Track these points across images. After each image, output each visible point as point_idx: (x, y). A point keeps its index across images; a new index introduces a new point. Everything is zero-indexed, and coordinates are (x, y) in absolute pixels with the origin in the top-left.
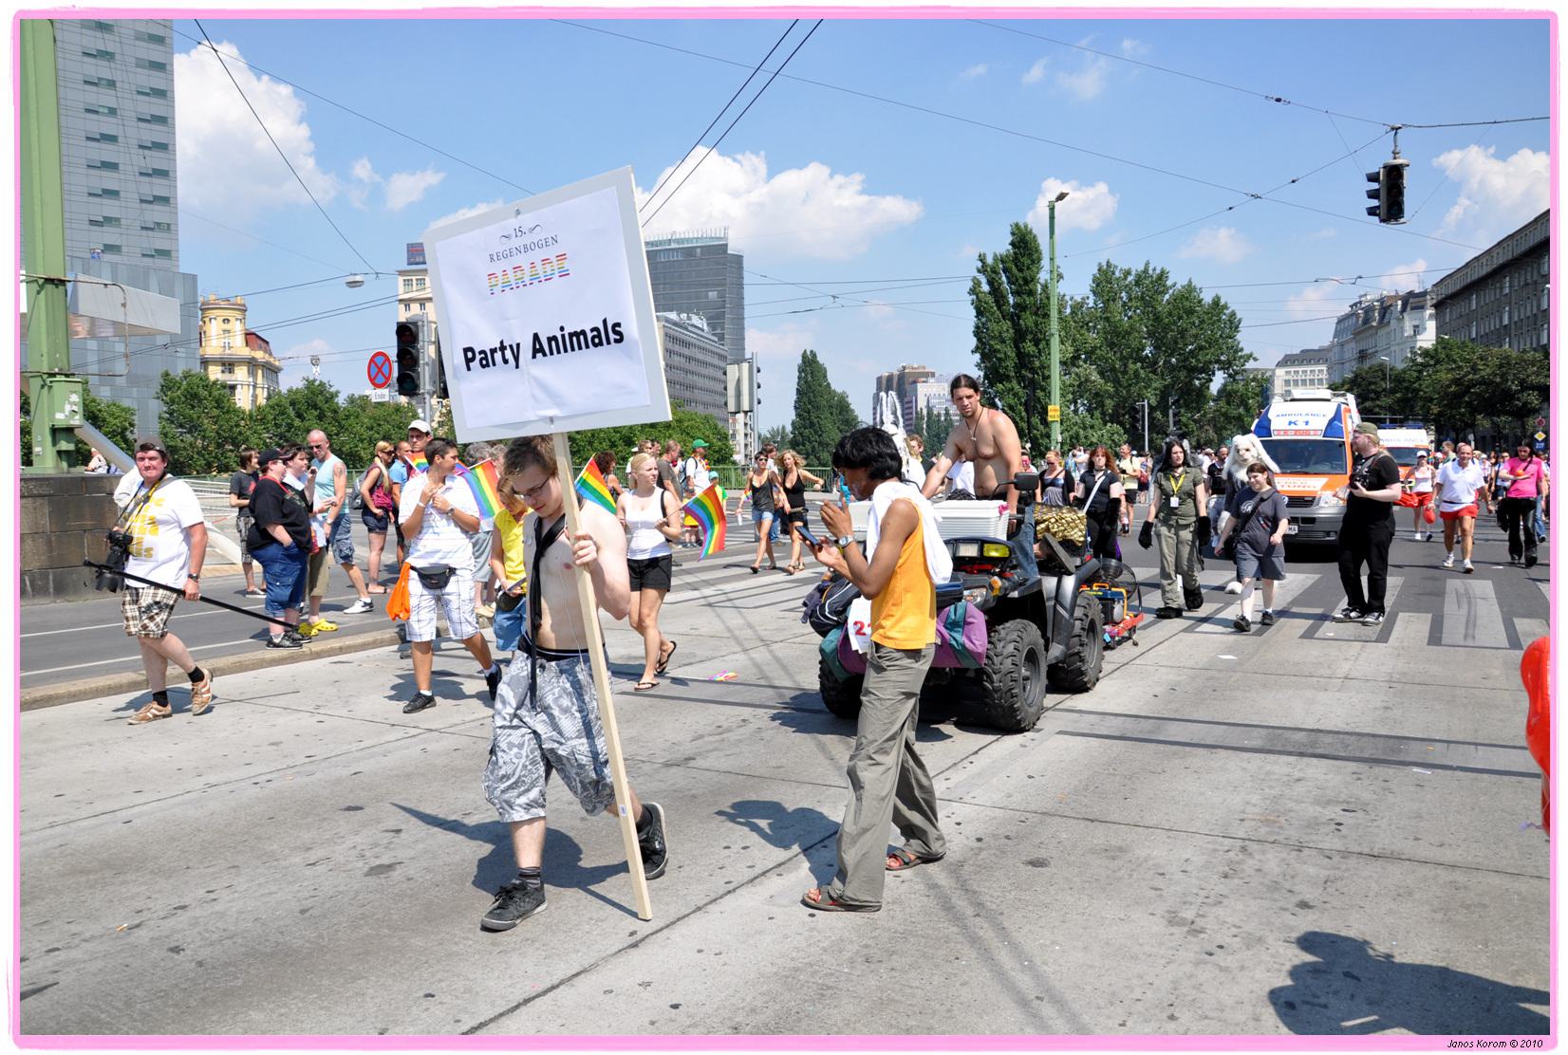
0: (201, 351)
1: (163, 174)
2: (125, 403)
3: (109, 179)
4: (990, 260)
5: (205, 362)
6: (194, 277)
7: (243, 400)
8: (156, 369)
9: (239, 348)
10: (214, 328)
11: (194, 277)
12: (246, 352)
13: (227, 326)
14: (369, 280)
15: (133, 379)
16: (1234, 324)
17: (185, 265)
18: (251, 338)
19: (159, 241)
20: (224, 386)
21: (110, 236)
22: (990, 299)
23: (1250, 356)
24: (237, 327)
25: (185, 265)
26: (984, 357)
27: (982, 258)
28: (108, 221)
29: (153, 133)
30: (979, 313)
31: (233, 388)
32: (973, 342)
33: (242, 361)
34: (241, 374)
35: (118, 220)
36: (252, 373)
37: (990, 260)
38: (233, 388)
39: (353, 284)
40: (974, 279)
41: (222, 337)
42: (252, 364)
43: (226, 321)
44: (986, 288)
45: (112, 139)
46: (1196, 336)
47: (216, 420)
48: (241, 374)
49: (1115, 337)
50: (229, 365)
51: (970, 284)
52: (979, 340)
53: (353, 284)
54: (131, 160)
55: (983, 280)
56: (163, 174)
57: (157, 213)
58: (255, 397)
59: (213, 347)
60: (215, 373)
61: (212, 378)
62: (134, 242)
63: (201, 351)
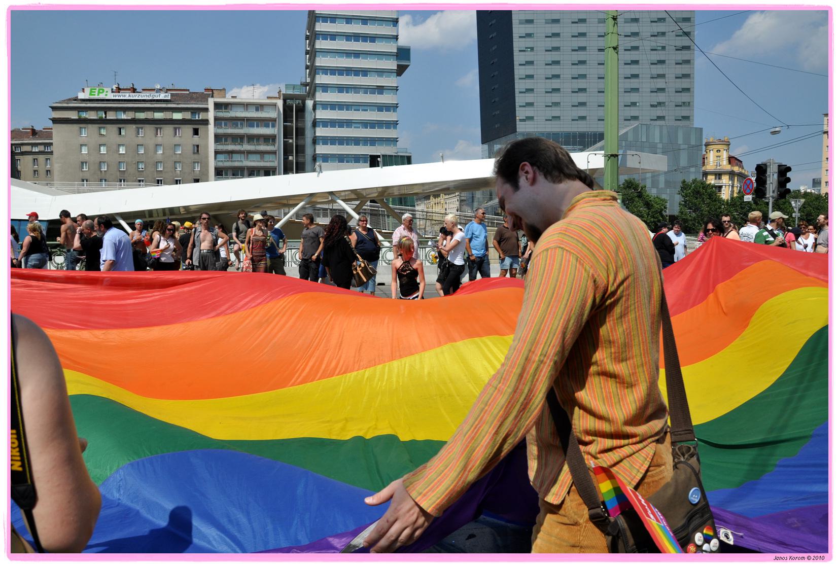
0: (703, 168)
1: (686, 76)
2: (663, 197)
3: (660, 83)
5: (706, 174)
6: (700, 130)
7: (725, 195)
8: (679, 178)
9: (725, 165)
10: (712, 156)
11: (700, 130)
12: (728, 168)
13: (718, 154)
15: (668, 183)
17: (697, 124)
18: (731, 160)
19: (684, 112)
20: (716, 187)
21: (659, 112)
24: (725, 155)
25: (697, 124)
28: (660, 104)
29: (685, 55)
31: (720, 187)
33: (725, 173)
34: (725, 180)
35: (664, 103)
36: (732, 179)
38: (720, 187)
41: (716, 159)
42: (732, 174)
43: (718, 151)
45: (662, 62)
47: (708, 205)
48: (725, 180)
50: (718, 175)
54: (671, 71)
56: (686, 76)
57: (684, 97)
58: (733, 192)
59: (711, 165)
60: (711, 180)
61: (708, 182)
62: (670, 113)
63: (703, 168)
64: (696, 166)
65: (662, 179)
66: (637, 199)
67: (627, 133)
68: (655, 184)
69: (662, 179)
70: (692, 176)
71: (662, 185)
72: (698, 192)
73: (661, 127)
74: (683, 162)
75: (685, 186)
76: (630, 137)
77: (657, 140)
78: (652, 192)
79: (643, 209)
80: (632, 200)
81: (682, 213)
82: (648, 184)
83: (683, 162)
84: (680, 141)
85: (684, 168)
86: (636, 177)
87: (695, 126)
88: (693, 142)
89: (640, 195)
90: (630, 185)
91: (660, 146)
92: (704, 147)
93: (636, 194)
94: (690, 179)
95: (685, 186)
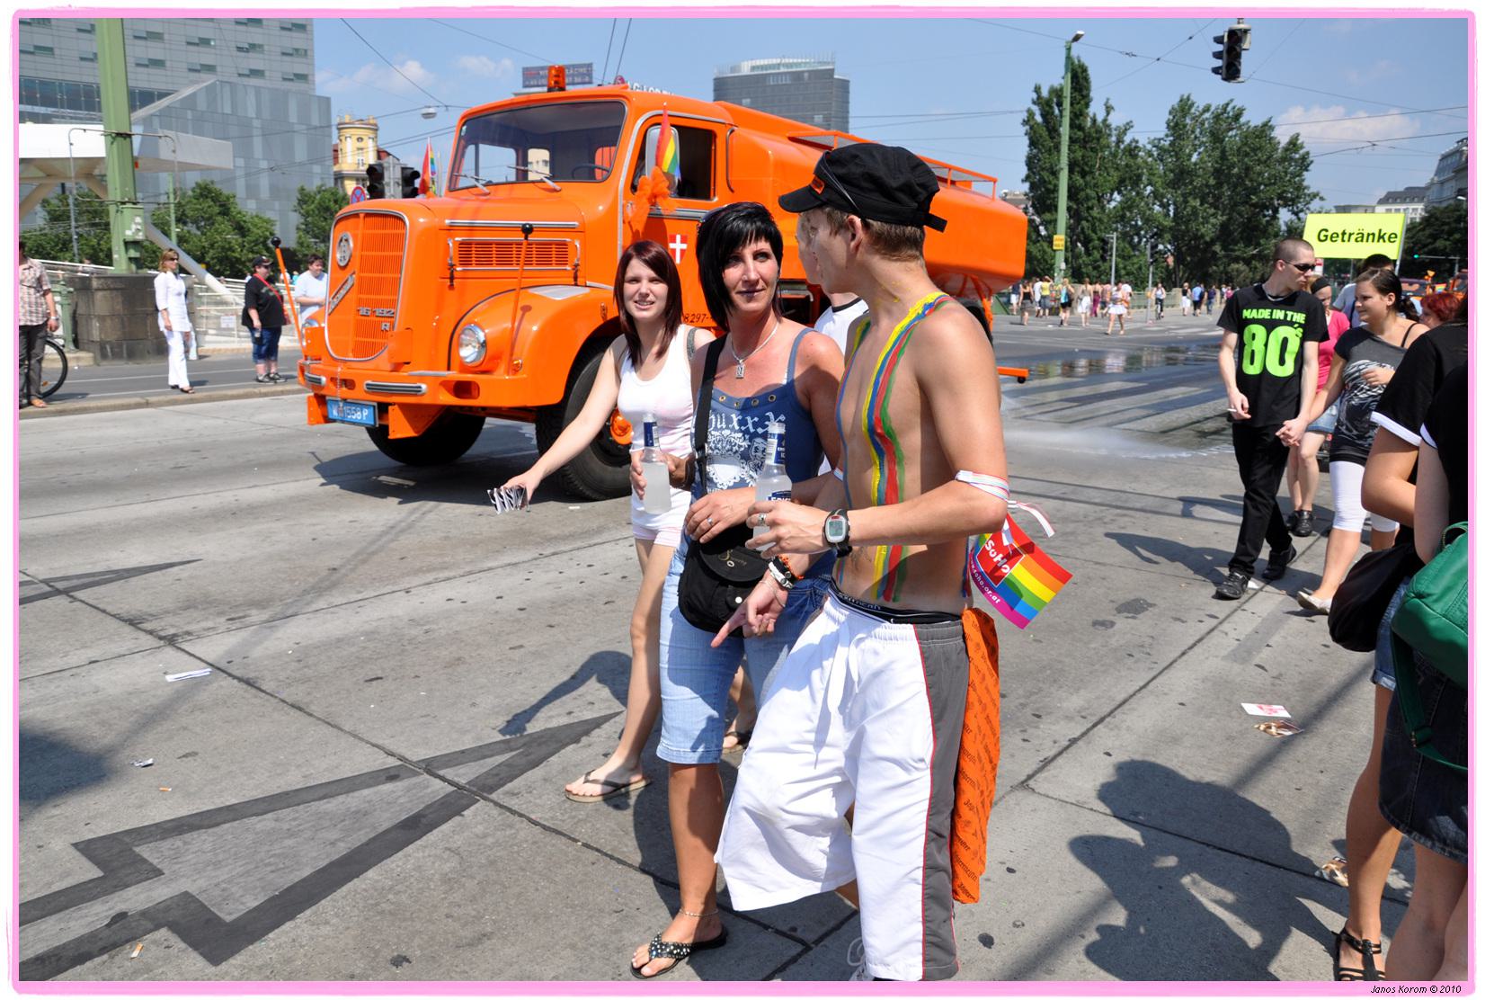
0: (336, 168)
2: (269, 215)
4: (1045, 93)
5: (340, 177)
6: (328, 100)
8: (295, 183)
10: (349, 146)
11: (328, 100)
13: (360, 145)
14: (441, 112)
15: (275, 191)
16: (1304, 164)
22: (1045, 134)
23: (1315, 196)
25: (320, 92)
26: (1032, 187)
27: (1037, 90)
30: (1033, 144)
32: (1024, 171)
37: (1045, 93)
39: (427, 116)
40: (1031, 114)
43: (360, 139)
44: (1039, 119)
46: (1260, 174)
49: (1181, 176)
51: (1025, 116)
52: (1030, 169)
53: (427, 116)
55: (1036, 109)
64: (319, 161)
65: (264, 182)
66: (219, 218)
67: (194, 95)
68: (252, 191)
69: (264, 182)
70: (317, 180)
71: (265, 193)
72: (327, 209)
73: (258, 90)
74: (300, 154)
75: (304, 199)
76: (202, 105)
77: (252, 113)
78: (247, 207)
79: (233, 238)
80: (210, 220)
81: (301, 244)
82: (240, 190)
83: (300, 154)
84: (293, 118)
85: (301, 164)
86: (216, 177)
87: (318, 93)
88: (315, 121)
89: (225, 211)
90: (205, 192)
91: (256, 123)
92: (335, 132)
93: (217, 209)
94: (313, 186)
95: (304, 199)
